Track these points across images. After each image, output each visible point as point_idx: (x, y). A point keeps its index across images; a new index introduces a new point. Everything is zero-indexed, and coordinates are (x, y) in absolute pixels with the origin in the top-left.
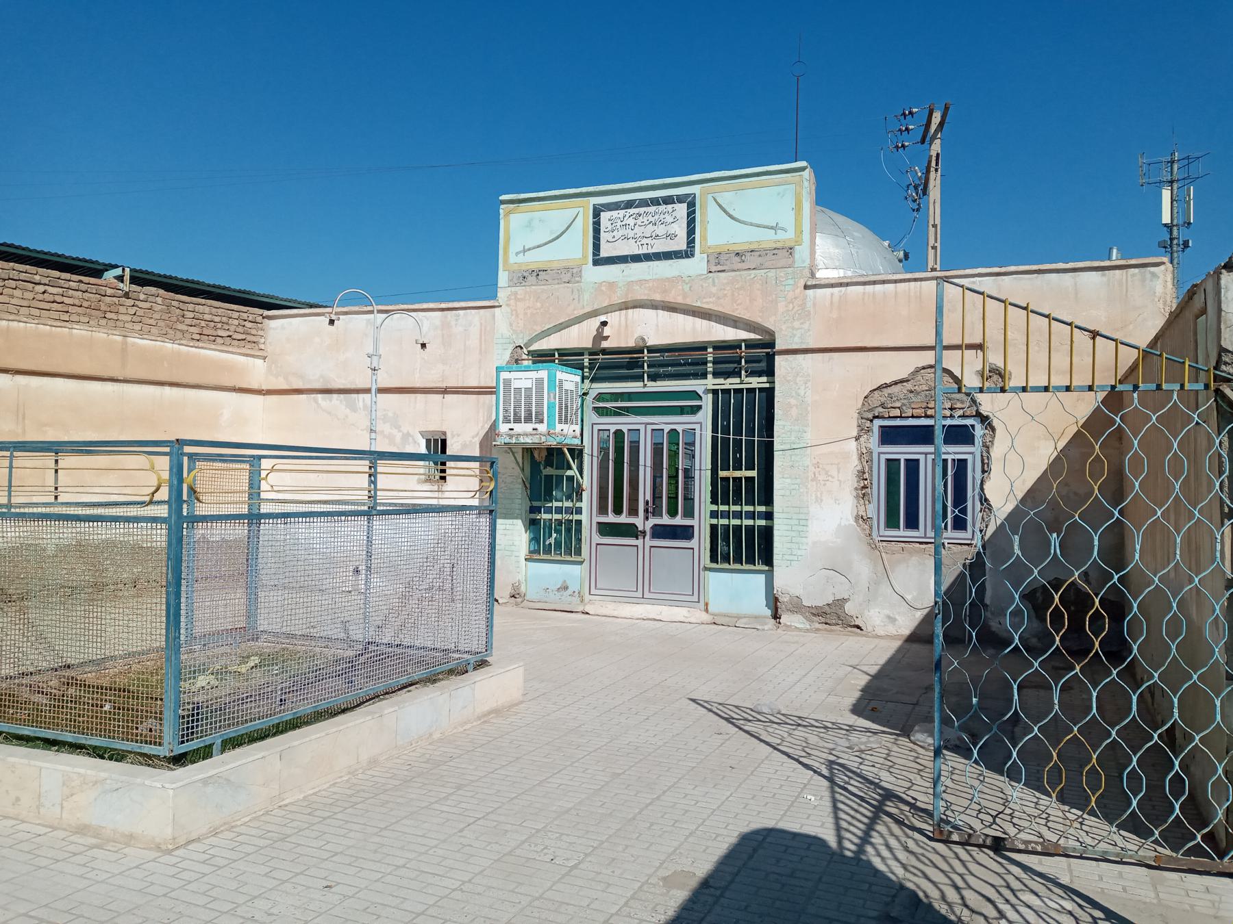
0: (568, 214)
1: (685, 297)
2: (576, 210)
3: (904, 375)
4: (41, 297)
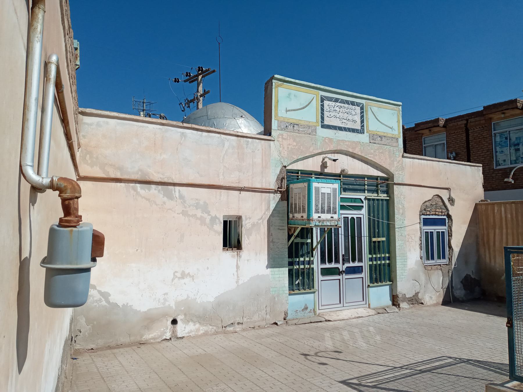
0: (309, 97)
1: (361, 153)
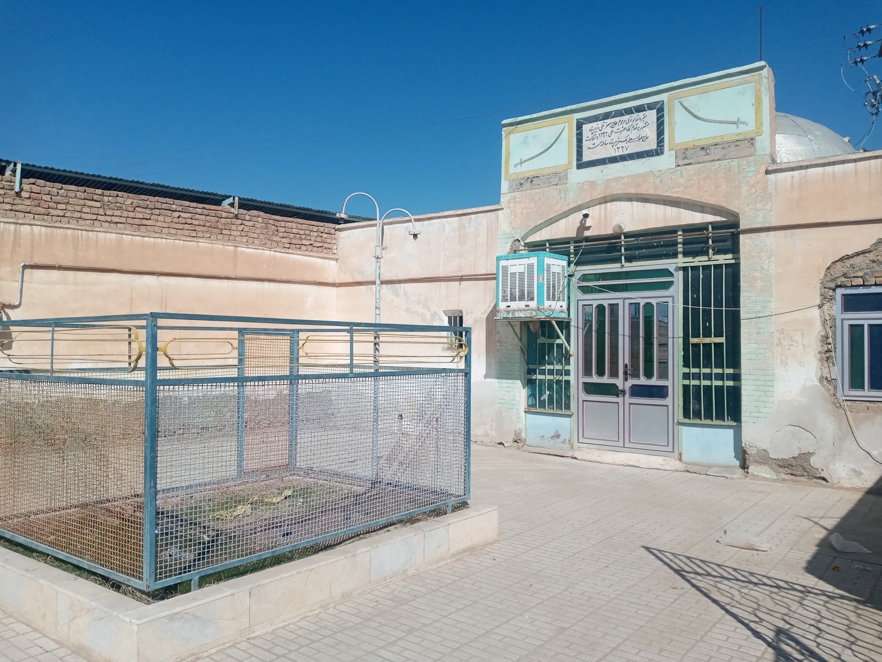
0: (557, 129)
2: (562, 126)
3: (866, 246)
4: (176, 220)
